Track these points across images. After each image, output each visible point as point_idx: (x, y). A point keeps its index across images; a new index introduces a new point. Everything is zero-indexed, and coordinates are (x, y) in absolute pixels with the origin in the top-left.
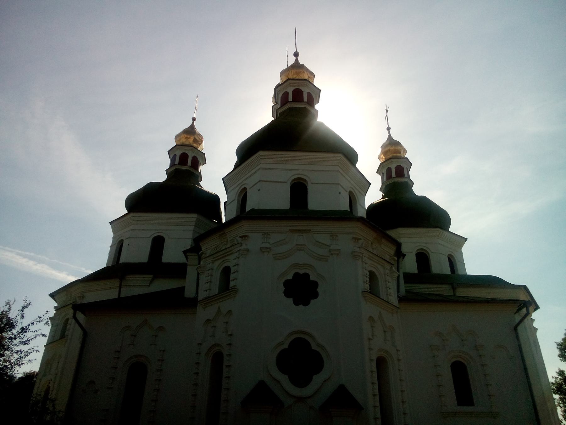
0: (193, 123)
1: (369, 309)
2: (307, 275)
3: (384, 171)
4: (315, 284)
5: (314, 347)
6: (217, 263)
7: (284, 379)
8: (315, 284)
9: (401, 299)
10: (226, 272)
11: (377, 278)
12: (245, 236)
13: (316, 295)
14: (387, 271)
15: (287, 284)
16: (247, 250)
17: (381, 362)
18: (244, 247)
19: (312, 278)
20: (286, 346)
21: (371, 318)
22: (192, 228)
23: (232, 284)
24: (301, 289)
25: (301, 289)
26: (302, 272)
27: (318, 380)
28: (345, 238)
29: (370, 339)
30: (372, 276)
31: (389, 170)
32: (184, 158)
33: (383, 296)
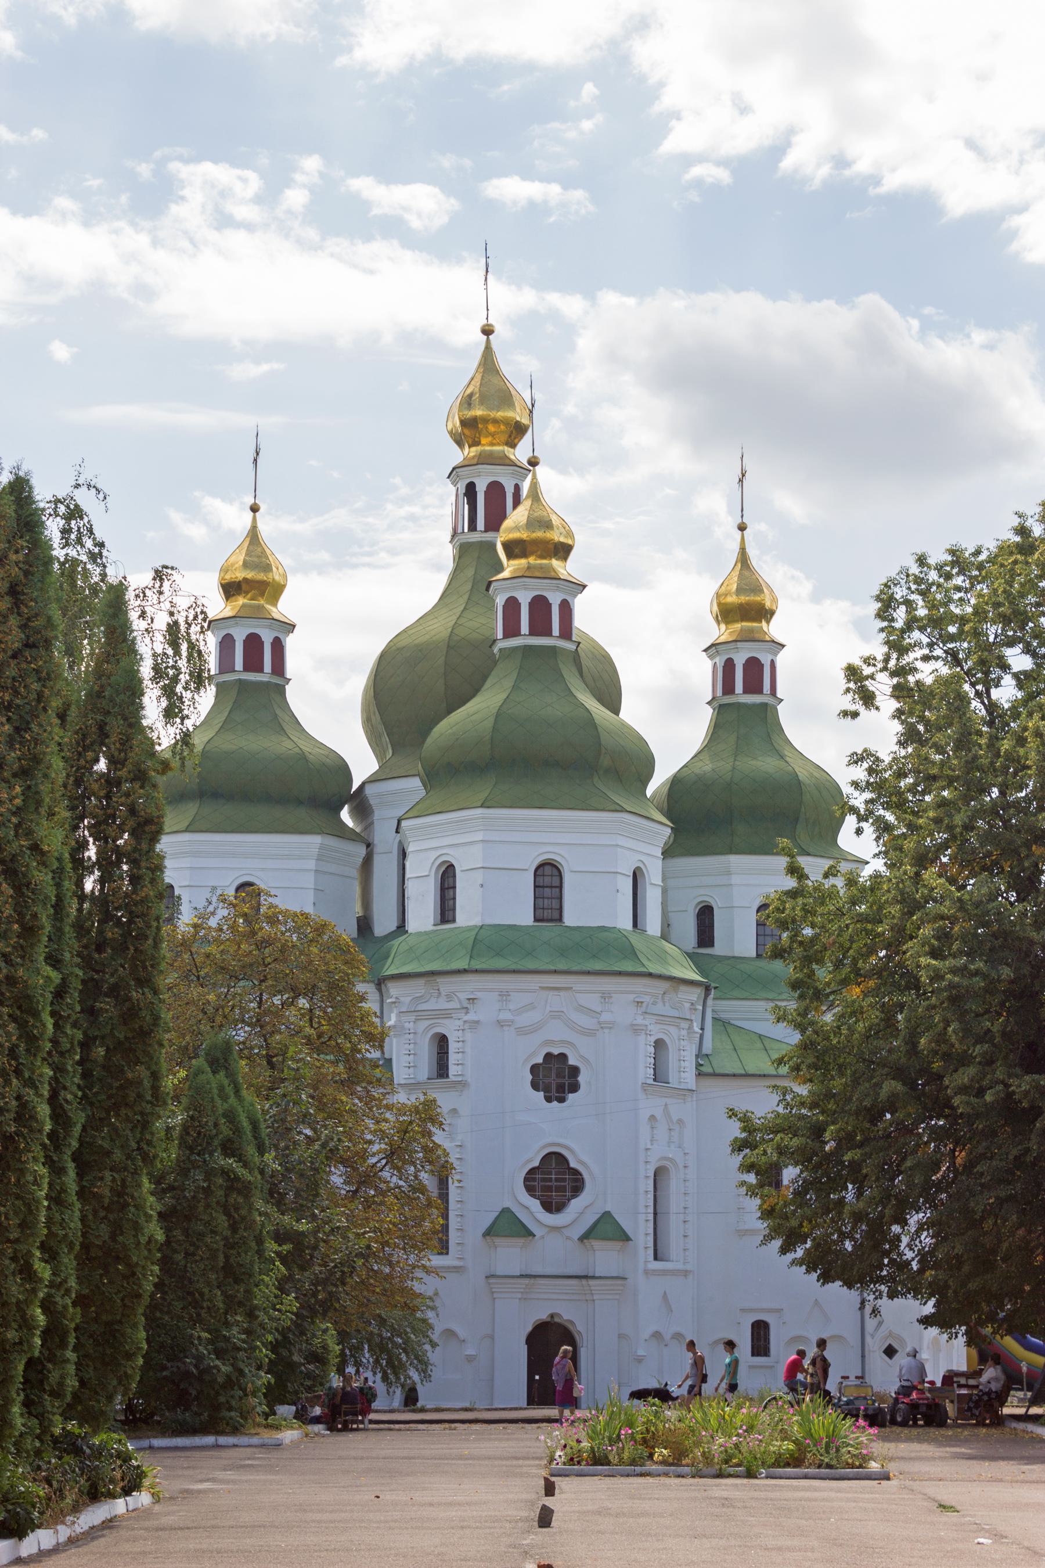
0: (254, 527)
1: (651, 1105)
2: (563, 1057)
3: (720, 661)
4: (575, 1071)
5: (573, 1164)
6: (423, 1025)
7: (535, 1205)
8: (575, 1071)
9: (700, 1074)
10: (442, 1043)
11: (667, 1048)
12: (473, 999)
13: (575, 1088)
14: (684, 1032)
15: (534, 1069)
16: (477, 1022)
17: (659, 1175)
18: (471, 1017)
19: (572, 1062)
20: (536, 1163)
21: (652, 1118)
22: (311, 864)
23: (453, 1070)
24: (556, 1078)
25: (556, 1078)
26: (556, 1052)
27: (576, 1205)
28: (621, 1002)
29: (647, 1149)
30: (659, 1045)
31: (729, 666)
32: (253, 642)
33: (674, 1082)
